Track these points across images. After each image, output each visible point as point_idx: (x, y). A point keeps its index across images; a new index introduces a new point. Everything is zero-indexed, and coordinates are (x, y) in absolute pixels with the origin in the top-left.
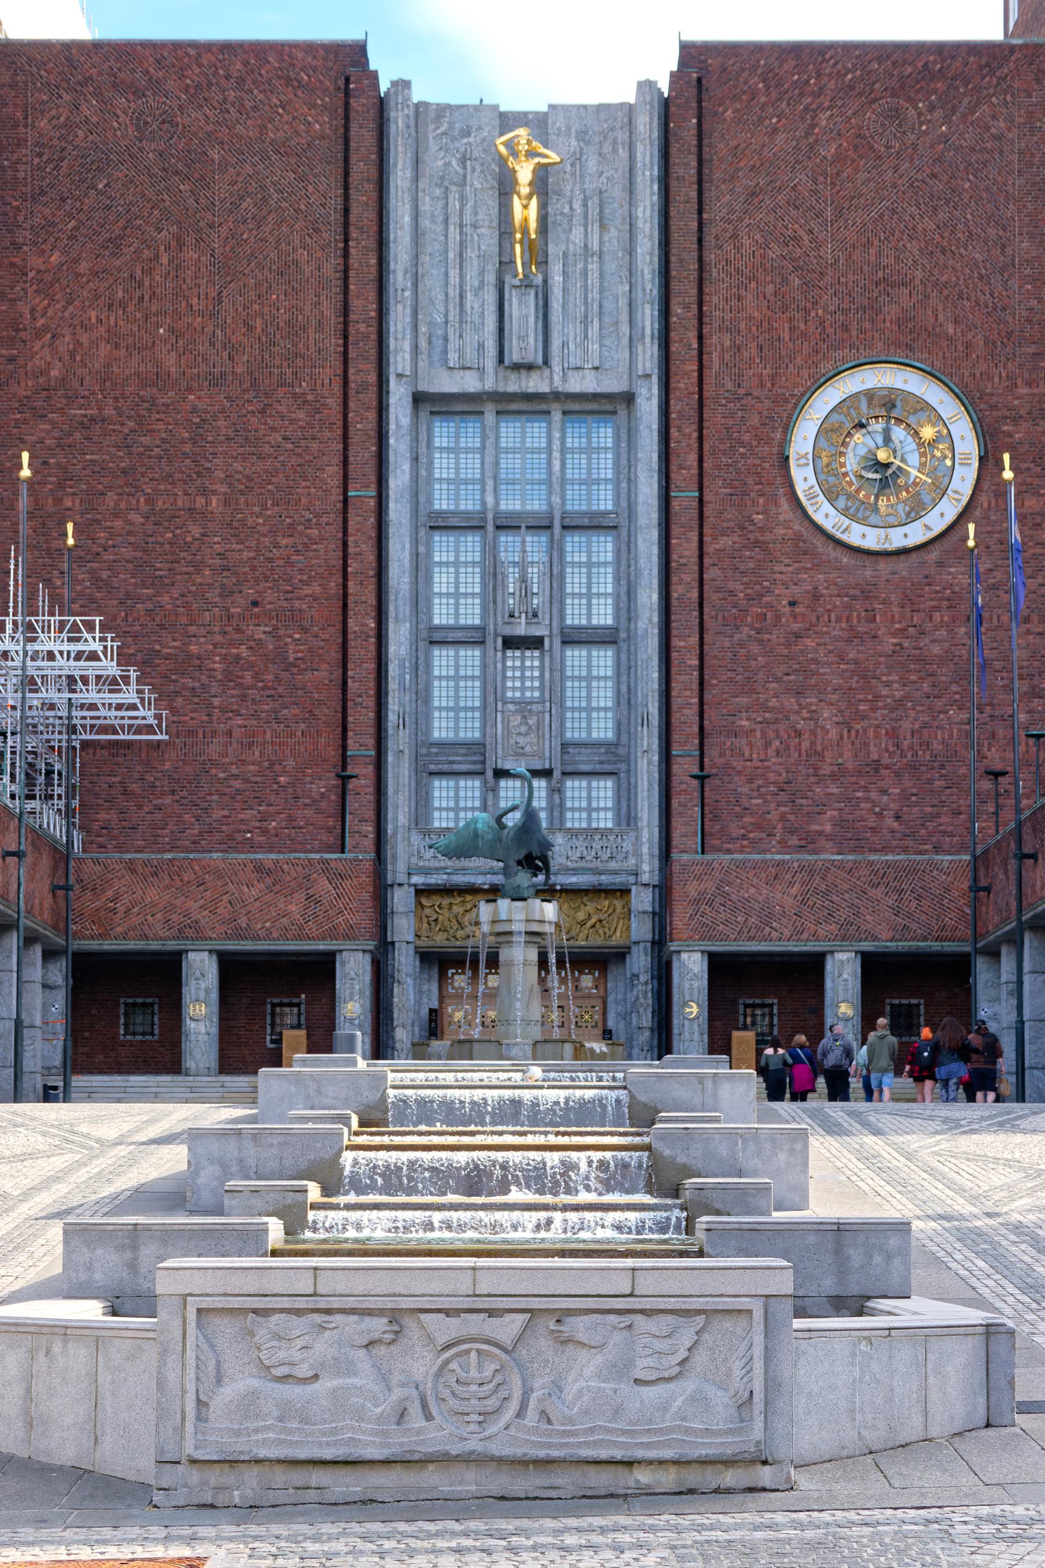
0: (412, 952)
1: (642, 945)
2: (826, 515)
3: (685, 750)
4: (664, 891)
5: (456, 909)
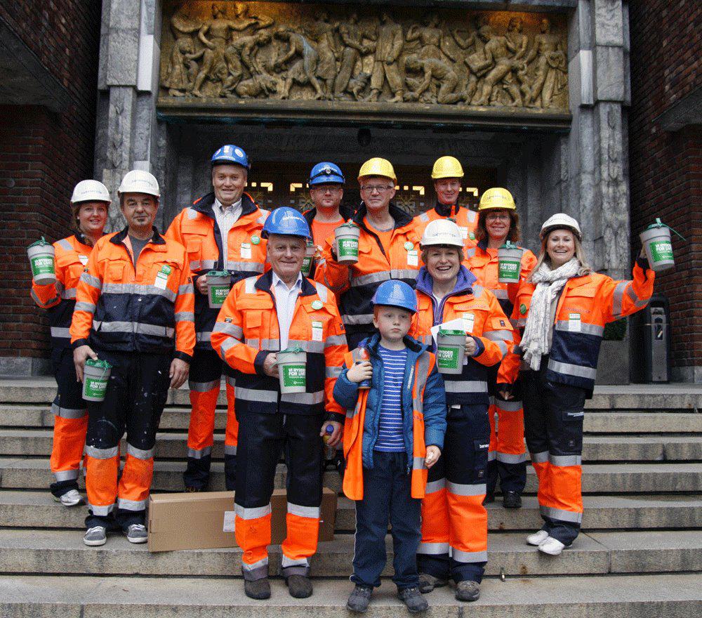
0: (147, 113)
1: (603, 110)
5: (239, 39)
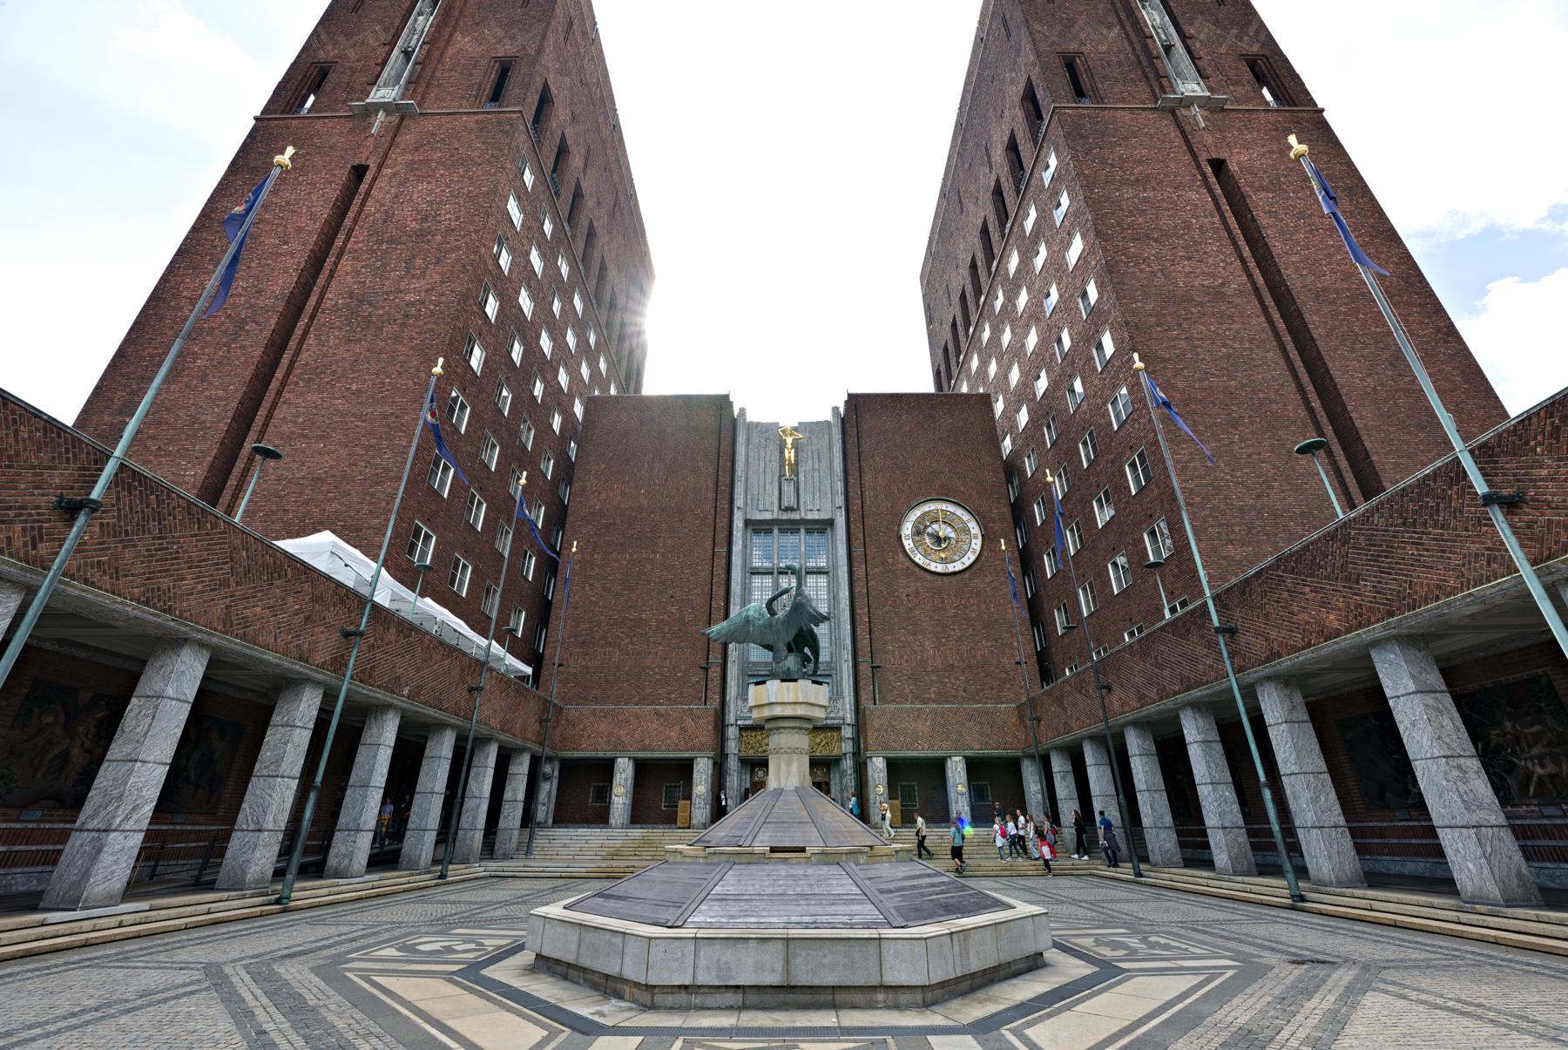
2: (919, 559)
3: (865, 660)
4: (859, 726)
